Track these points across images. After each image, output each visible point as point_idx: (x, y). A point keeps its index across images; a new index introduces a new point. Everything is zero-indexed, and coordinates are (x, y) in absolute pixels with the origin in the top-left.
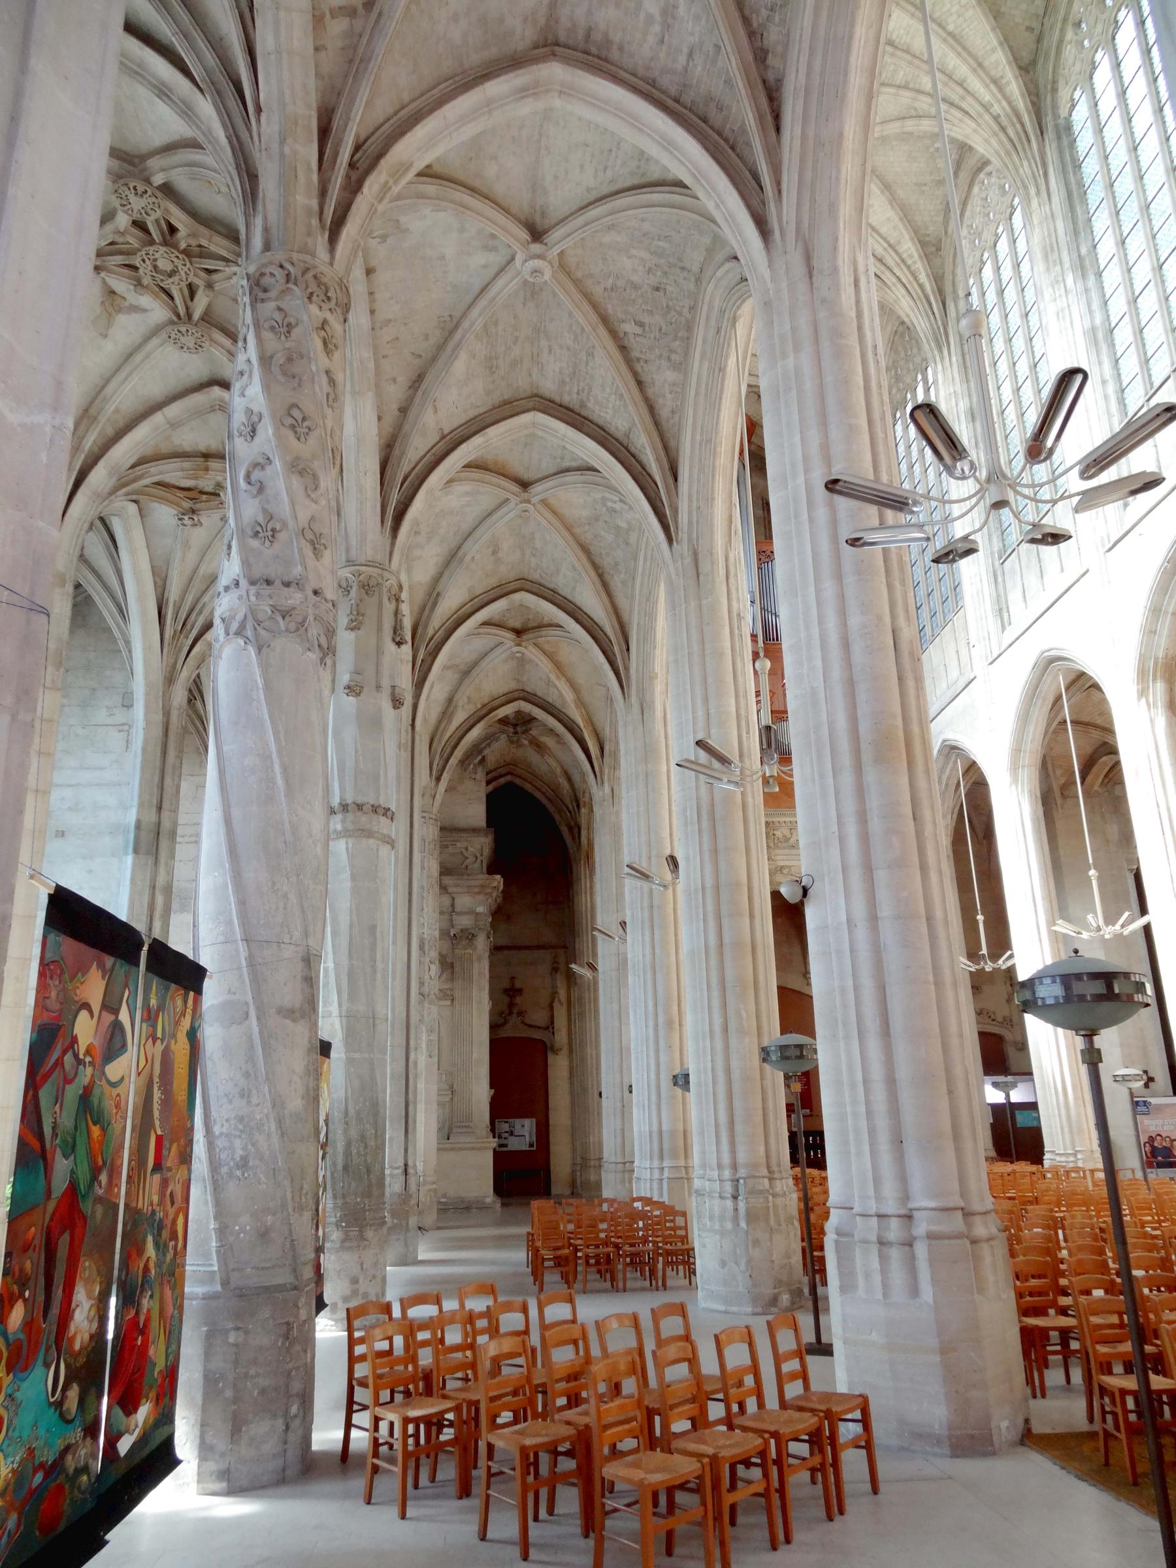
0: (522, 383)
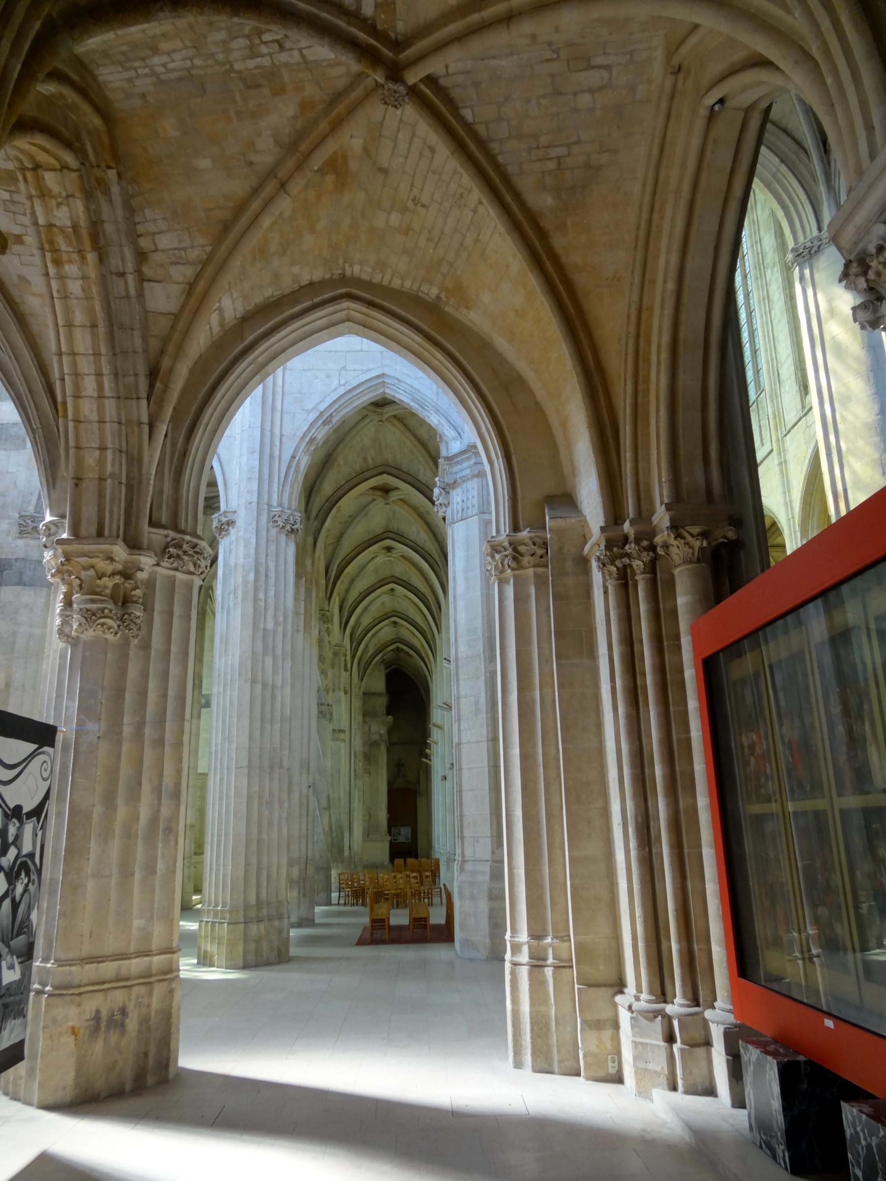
0: (388, 573)
